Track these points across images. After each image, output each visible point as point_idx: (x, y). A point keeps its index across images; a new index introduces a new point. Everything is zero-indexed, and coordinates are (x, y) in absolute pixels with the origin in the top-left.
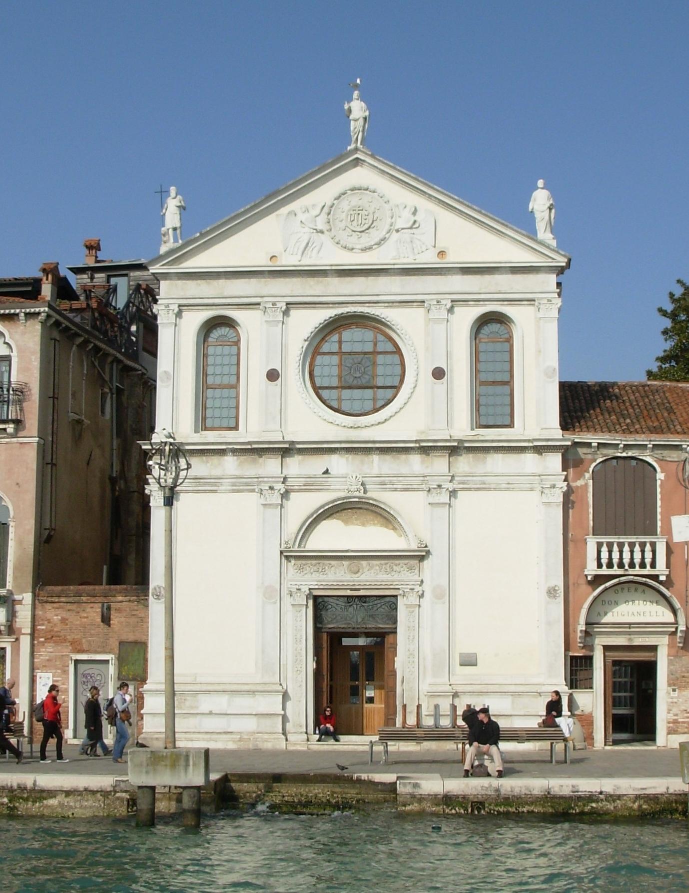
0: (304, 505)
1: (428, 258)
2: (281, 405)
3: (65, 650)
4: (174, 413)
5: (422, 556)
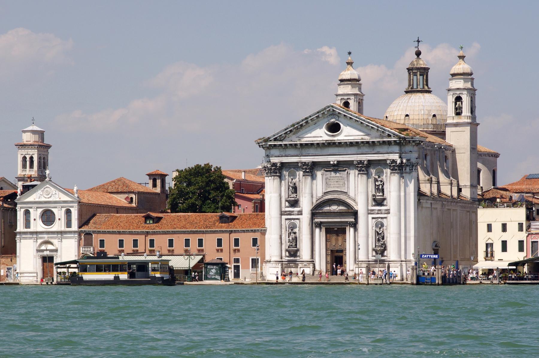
0: (40, 241)
1: (58, 200)
2: (38, 225)
3: (5, 266)
4: (20, 227)
5: (56, 251)
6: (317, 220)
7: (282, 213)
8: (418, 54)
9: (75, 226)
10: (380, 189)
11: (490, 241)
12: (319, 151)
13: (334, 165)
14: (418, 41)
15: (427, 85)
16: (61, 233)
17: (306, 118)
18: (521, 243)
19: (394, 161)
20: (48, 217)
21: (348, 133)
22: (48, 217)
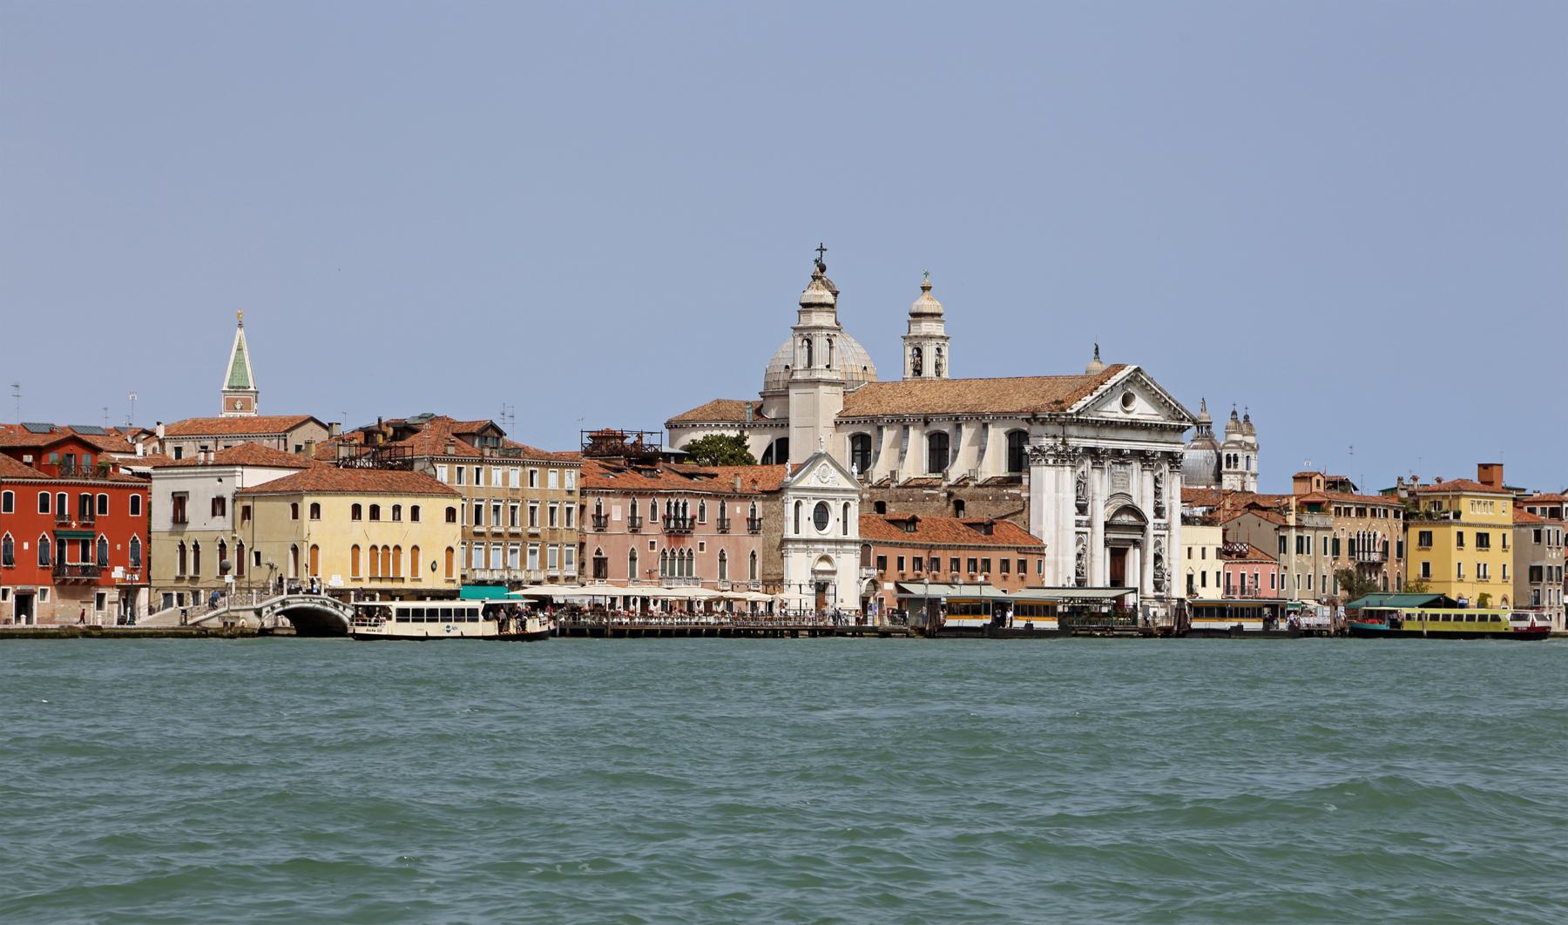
0: (816, 556)
2: (808, 530)
5: (834, 573)
9: (854, 533)
16: (837, 542)
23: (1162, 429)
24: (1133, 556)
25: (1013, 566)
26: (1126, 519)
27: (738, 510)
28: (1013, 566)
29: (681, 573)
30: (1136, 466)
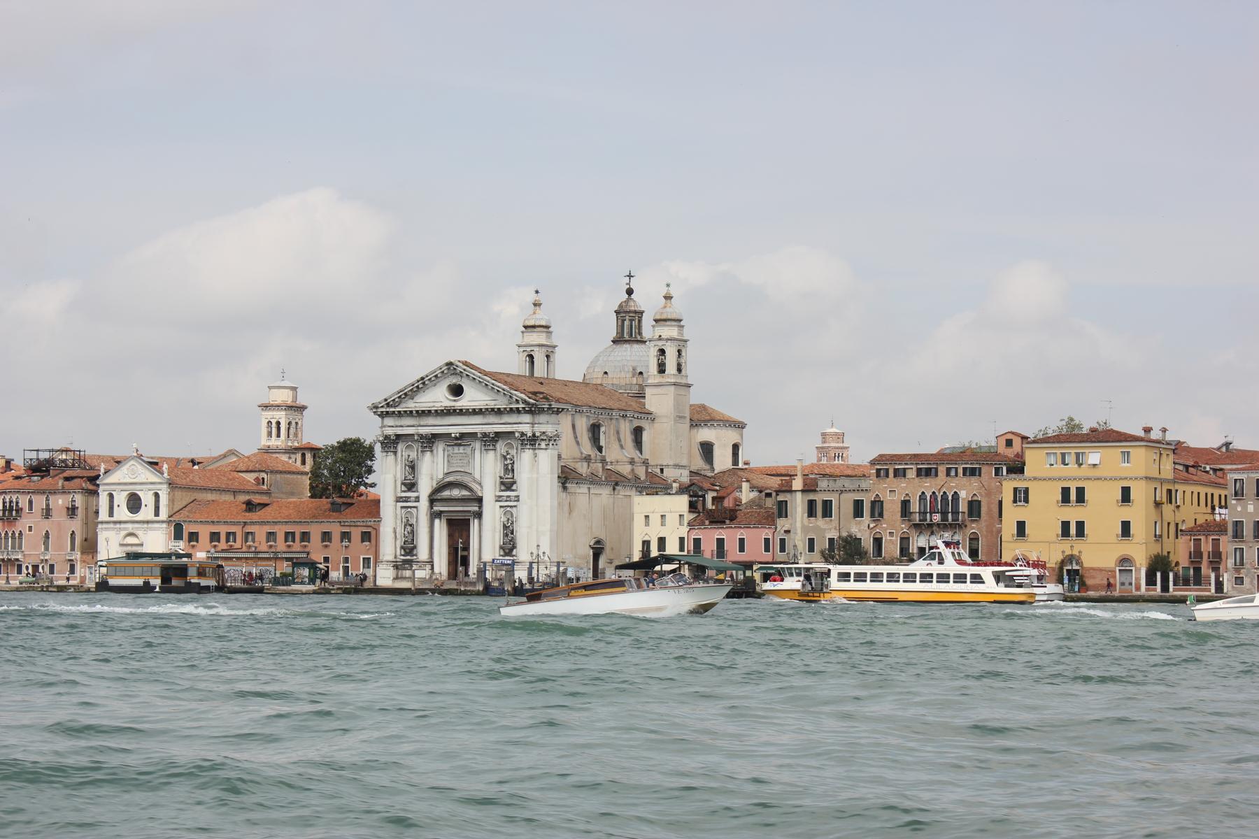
0: (124, 533)
2: (122, 512)
4: (103, 515)
6: (435, 508)
7: (399, 500)
8: (630, 292)
9: (164, 515)
10: (509, 469)
11: (647, 538)
12: (439, 421)
13: (456, 438)
14: (630, 276)
15: (640, 333)
17: (422, 378)
18: (682, 540)
19: (523, 434)
20: (134, 503)
21: (473, 397)
22: (134, 503)
23: (498, 412)
24: (474, 526)
25: (336, 537)
26: (456, 493)
27: (60, 502)
28: (336, 537)
29: (13, 547)
30: (477, 445)
